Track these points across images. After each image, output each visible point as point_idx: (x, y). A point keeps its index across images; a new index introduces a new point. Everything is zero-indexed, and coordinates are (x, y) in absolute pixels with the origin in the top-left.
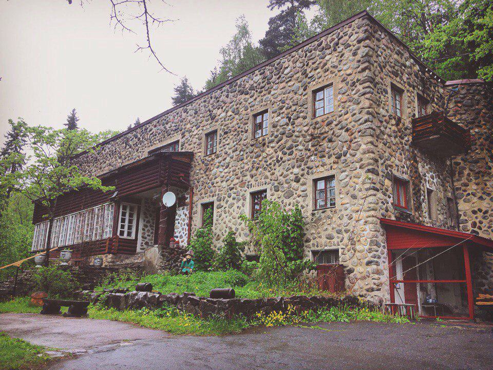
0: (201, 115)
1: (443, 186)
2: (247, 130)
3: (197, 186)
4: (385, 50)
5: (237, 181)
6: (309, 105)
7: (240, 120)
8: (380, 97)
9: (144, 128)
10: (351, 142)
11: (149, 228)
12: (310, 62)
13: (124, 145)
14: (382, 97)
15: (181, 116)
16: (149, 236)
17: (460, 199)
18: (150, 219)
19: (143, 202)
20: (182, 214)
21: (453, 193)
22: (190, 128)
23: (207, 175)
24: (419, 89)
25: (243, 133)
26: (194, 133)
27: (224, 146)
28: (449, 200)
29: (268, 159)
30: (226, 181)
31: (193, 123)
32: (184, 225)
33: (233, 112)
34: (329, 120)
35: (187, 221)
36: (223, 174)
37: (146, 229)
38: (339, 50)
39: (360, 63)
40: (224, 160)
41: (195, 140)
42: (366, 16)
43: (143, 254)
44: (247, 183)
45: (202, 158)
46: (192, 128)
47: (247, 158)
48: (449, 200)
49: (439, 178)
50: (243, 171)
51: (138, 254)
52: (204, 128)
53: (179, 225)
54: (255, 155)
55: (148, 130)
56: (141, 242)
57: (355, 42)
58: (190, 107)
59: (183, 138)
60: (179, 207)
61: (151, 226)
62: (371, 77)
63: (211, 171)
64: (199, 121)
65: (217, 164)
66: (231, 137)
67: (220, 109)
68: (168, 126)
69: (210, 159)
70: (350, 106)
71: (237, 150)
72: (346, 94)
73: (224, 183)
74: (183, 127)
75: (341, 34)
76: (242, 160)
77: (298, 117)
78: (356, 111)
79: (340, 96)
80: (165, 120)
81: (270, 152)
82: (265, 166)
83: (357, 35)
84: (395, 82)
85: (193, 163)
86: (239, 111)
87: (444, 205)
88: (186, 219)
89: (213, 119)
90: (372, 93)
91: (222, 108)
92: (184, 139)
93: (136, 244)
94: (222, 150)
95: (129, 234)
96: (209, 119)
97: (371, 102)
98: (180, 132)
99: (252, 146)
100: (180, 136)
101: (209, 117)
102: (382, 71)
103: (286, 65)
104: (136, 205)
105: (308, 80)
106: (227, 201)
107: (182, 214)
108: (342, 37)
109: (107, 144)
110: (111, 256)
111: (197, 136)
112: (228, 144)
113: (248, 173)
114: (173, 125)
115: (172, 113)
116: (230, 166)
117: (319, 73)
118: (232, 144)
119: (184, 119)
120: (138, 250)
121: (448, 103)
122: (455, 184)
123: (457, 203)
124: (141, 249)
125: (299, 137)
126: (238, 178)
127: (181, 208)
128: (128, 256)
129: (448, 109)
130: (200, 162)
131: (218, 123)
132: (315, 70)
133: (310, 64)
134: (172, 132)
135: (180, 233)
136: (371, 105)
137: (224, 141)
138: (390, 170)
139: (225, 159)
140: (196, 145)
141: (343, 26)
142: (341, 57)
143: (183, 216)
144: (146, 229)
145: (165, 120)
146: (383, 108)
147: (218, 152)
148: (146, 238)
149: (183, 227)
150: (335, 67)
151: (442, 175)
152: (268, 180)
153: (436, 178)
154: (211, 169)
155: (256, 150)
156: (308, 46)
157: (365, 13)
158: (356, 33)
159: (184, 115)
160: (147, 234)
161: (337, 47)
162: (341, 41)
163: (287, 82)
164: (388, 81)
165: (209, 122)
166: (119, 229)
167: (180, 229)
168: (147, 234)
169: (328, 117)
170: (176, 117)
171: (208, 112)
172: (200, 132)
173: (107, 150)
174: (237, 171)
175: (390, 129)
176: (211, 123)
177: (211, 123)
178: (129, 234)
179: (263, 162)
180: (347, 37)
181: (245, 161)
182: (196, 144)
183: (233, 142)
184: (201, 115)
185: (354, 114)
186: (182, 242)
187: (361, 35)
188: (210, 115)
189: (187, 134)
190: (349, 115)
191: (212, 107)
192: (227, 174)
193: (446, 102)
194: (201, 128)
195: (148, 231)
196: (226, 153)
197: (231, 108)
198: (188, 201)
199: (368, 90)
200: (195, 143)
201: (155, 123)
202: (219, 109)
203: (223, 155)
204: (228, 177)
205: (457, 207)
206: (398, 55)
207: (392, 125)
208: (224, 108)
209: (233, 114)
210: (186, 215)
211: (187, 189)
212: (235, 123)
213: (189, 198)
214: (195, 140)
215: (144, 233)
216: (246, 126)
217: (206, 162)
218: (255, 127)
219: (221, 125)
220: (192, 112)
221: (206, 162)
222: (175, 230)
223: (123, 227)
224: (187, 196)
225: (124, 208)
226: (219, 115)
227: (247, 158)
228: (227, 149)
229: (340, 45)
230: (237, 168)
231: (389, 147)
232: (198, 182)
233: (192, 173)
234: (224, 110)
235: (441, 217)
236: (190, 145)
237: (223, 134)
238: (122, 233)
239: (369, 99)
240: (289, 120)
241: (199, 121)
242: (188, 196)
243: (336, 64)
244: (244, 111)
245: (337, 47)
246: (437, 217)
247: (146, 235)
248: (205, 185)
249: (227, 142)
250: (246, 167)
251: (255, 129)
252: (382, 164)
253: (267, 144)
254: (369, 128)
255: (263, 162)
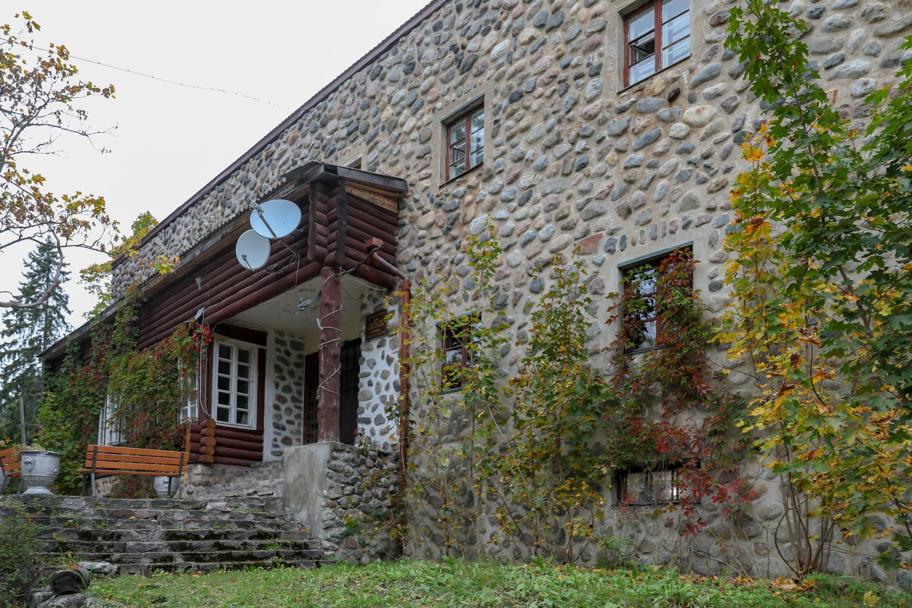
0: (427, 70)
2: (600, 66)
3: (421, 276)
5: (567, 236)
7: (568, 42)
9: (264, 153)
11: (290, 404)
13: (220, 208)
15: (362, 94)
16: (291, 422)
18: (289, 381)
19: (270, 339)
20: (378, 358)
22: (395, 118)
23: (454, 238)
25: (581, 81)
26: (406, 128)
27: (509, 138)
29: (694, 140)
30: (524, 245)
31: (402, 99)
32: (387, 388)
33: (541, 26)
35: (394, 377)
36: (510, 224)
37: (283, 407)
40: (510, 183)
41: (408, 147)
43: (280, 466)
44: (605, 239)
45: (435, 192)
46: (399, 114)
47: (601, 156)
50: (588, 201)
51: (267, 464)
52: (439, 105)
53: (373, 389)
54: (634, 141)
55: (275, 156)
56: (273, 436)
58: (391, 58)
59: (370, 151)
60: (368, 340)
61: (294, 399)
63: (466, 223)
64: (419, 91)
65: (489, 198)
66: (535, 105)
67: (493, 33)
68: (325, 133)
69: (462, 188)
71: (558, 142)
73: (516, 251)
74: (371, 121)
76: (583, 166)
80: (319, 116)
81: (706, 114)
82: (683, 167)
85: (405, 212)
86: (563, 16)
88: (391, 369)
89: (466, 69)
91: (498, 28)
92: (375, 153)
93: (261, 441)
94: (503, 154)
95: (241, 416)
96: (453, 73)
98: (360, 140)
99: (622, 111)
100: (364, 148)
101: (455, 67)
104: (253, 348)
106: (529, 305)
107: (378, 358)
109: (180, 216)
110: (199, 468)
111: (415, 135)
112: (525, 130)
113: (609, 206)
114: (343, 122)
115: (337, 93)
116: (537, 194)
118: (539, 128)
119: (373, 97)
120: (267, 454)
124: (273, 453)
125: (845, 26)
126: (567, 229)
127: (375, 343)
128: (243, 470)
130: (428, 206)
131: (482, 79)
134: (339, 145)
135: (374, 409)
137: (510, 123)
139: (517, 177)
140: (412, 161)
143: (382, 365)
144: (283, 407)
145: (319, 116)
147: (488, 164)
148: (284, 429)
149: (383, 392)
152: (695, 215)
154: (468, 218)
155: (640, 122)
159: (372, 87)
160: (285, 418)
165: (453, 83)
166: (215, 404)
167: (376, 400)
168: (285, 418)
170: (350, 99)
171: (451, 55)
172: (425, 119)
173: (184, 230)
174: (564, 204)
176: (461, 83)
177: (461, 83)
178: (241, 416)
179: (673, 159)
181: (593, 169)
182: (414, 157)
183: (546, 118)
184: (427, 70)
186: (383, 433)
188: (458, 61)
189: (384, 140)
191: (463, 35)
192: (527, 222)
194: (427, 107)
195: (289, 411)
196: (520, 159)
197: (530, 16)
198: (393, 320)
200: (408, 157)
201: (290, 134)
202: (486, 33)
203: (509, 165)
204: (530, 232)
208: (505, 24)
209: (541, 35)
210: (390, 361)
211: (390, 288)
212: (548, 58)
213: (397, 313)
214: (408, 147)
215: (279, 417)
216: (595, 54)
217: (448, 201)
218: (626, 52)
219: (498, 80)
220: (398, 72)
221: (448, 201)
222: (362, 404)
223: (224, 399)
224: (390, 308)
225: (225, 352)
226: (489, 51)
227: (601, 156)
228: (522, 147)
230: (562, 197)
232: (425, 264)
233: (404, 242)
234: (507, 31)
236: (393, 164)
237: (505, 102)
238: (223, 415)
241: (419, 91)
242: (395, 307)
244: (584, 11)
247: (283, 422)
248: (447, 267)
249: (523, 124)
250: (602, 185)
251: (626, 58)
253: (686, 92)
255: (673, 159)
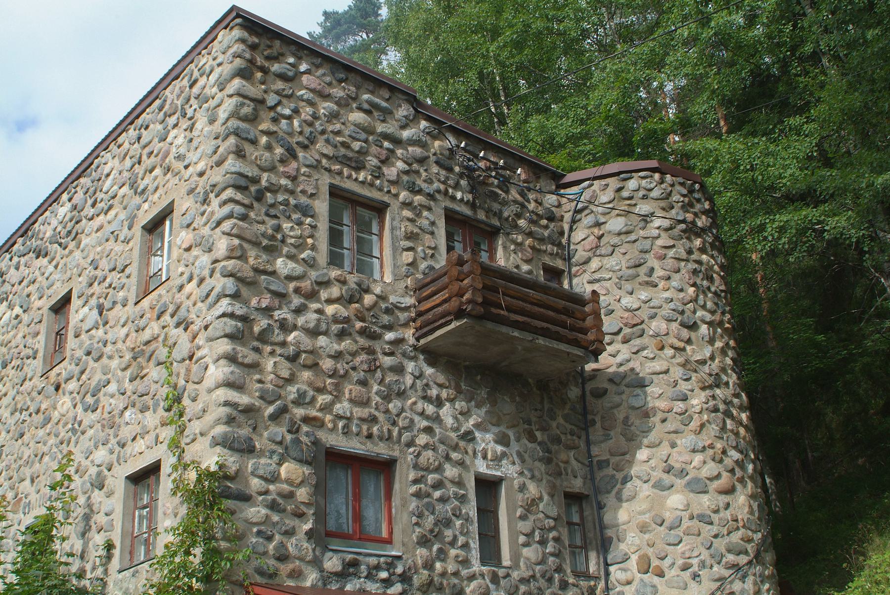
1: (548, 461)
4: (311, 103)
6: (133, 270)
8: (278, 229)
10: (191, 358)
12: (147, 150)
14: (286, 225)
17: (609, 492)
21: (591, 477)
24: (453, 198)
28: (573, 499)
34: (163, 301)
38: (190, 112)
39: (219, 141)
42: (238, 20)
48: (573, 499)
49: (532, 438)
57: (215, 89)
62: (241, 174)
70: (196, 257)
72: (192, 227)
75: (196, 74)
77: (115, 303)
78: (206, 273)
79: (183, 233)
83: (220, 68)
84: (348, 185)
87: (548, 517)
90: (244, 218)
97: (236, 242)
102: (295, 157)
103: (107, 169)
105: (137, 200)
108: (196, 81)
117: (156, 178)
121: (571, 230)
122: (595, 450)
123: (601, 507)
129: (572, 247)
132: (151, 172)
133: (144, 157)
136: (232, 249)
138: (307, 434)
141: (200, 54)
142: (191, 131)
146: (291, 257)
150: (180, 157)
151: (543, 429)
153: (518, 440)
156: (144, 115)
157: (234, 14)
158: (219, 65)
161: (187, 107)
162: (196, 90)
163: (106, 214)
164: (326, 180)
169: (160, 296)
175: (320, 312)
180: (205, 77)
185: (202, 281)
187: (227, 69)
190: (195, 282)
193: (566, 227)
199: (227, 209)
205: (601, 520)
206: (368, 112)
207: (329, 301)
229: (193, 101)
231: (314, 367)
235: (530, 553)
239: (228, 234)
240: (101, 314)
243: (182, 150)
245: (187, 107)
246: (516, 557)
252: (274, 417)
254: (224, 315)
